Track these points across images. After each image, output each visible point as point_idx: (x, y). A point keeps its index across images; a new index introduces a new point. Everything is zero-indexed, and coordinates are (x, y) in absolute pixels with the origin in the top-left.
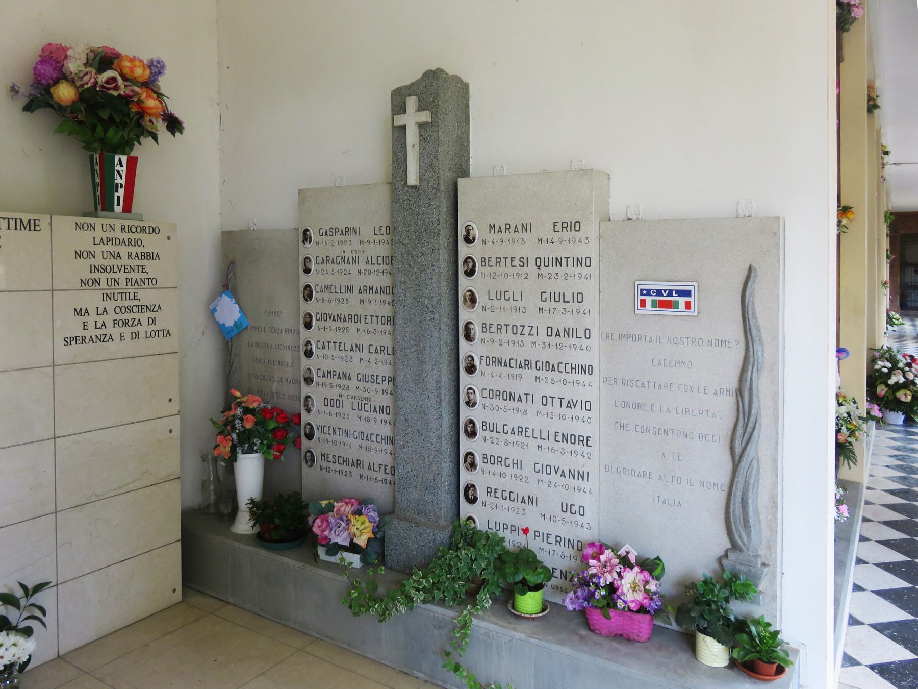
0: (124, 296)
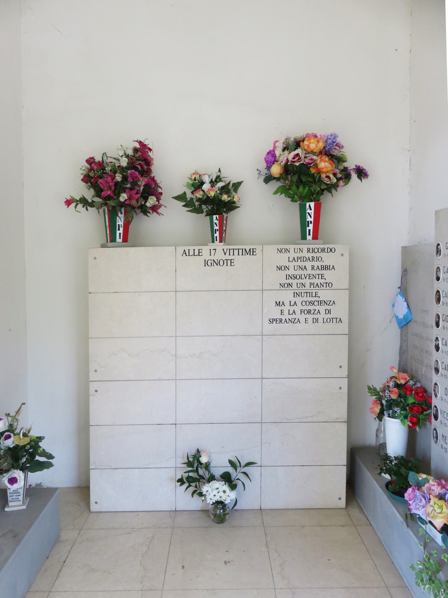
0: (308, 294)
